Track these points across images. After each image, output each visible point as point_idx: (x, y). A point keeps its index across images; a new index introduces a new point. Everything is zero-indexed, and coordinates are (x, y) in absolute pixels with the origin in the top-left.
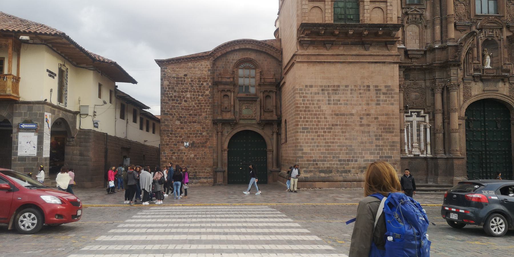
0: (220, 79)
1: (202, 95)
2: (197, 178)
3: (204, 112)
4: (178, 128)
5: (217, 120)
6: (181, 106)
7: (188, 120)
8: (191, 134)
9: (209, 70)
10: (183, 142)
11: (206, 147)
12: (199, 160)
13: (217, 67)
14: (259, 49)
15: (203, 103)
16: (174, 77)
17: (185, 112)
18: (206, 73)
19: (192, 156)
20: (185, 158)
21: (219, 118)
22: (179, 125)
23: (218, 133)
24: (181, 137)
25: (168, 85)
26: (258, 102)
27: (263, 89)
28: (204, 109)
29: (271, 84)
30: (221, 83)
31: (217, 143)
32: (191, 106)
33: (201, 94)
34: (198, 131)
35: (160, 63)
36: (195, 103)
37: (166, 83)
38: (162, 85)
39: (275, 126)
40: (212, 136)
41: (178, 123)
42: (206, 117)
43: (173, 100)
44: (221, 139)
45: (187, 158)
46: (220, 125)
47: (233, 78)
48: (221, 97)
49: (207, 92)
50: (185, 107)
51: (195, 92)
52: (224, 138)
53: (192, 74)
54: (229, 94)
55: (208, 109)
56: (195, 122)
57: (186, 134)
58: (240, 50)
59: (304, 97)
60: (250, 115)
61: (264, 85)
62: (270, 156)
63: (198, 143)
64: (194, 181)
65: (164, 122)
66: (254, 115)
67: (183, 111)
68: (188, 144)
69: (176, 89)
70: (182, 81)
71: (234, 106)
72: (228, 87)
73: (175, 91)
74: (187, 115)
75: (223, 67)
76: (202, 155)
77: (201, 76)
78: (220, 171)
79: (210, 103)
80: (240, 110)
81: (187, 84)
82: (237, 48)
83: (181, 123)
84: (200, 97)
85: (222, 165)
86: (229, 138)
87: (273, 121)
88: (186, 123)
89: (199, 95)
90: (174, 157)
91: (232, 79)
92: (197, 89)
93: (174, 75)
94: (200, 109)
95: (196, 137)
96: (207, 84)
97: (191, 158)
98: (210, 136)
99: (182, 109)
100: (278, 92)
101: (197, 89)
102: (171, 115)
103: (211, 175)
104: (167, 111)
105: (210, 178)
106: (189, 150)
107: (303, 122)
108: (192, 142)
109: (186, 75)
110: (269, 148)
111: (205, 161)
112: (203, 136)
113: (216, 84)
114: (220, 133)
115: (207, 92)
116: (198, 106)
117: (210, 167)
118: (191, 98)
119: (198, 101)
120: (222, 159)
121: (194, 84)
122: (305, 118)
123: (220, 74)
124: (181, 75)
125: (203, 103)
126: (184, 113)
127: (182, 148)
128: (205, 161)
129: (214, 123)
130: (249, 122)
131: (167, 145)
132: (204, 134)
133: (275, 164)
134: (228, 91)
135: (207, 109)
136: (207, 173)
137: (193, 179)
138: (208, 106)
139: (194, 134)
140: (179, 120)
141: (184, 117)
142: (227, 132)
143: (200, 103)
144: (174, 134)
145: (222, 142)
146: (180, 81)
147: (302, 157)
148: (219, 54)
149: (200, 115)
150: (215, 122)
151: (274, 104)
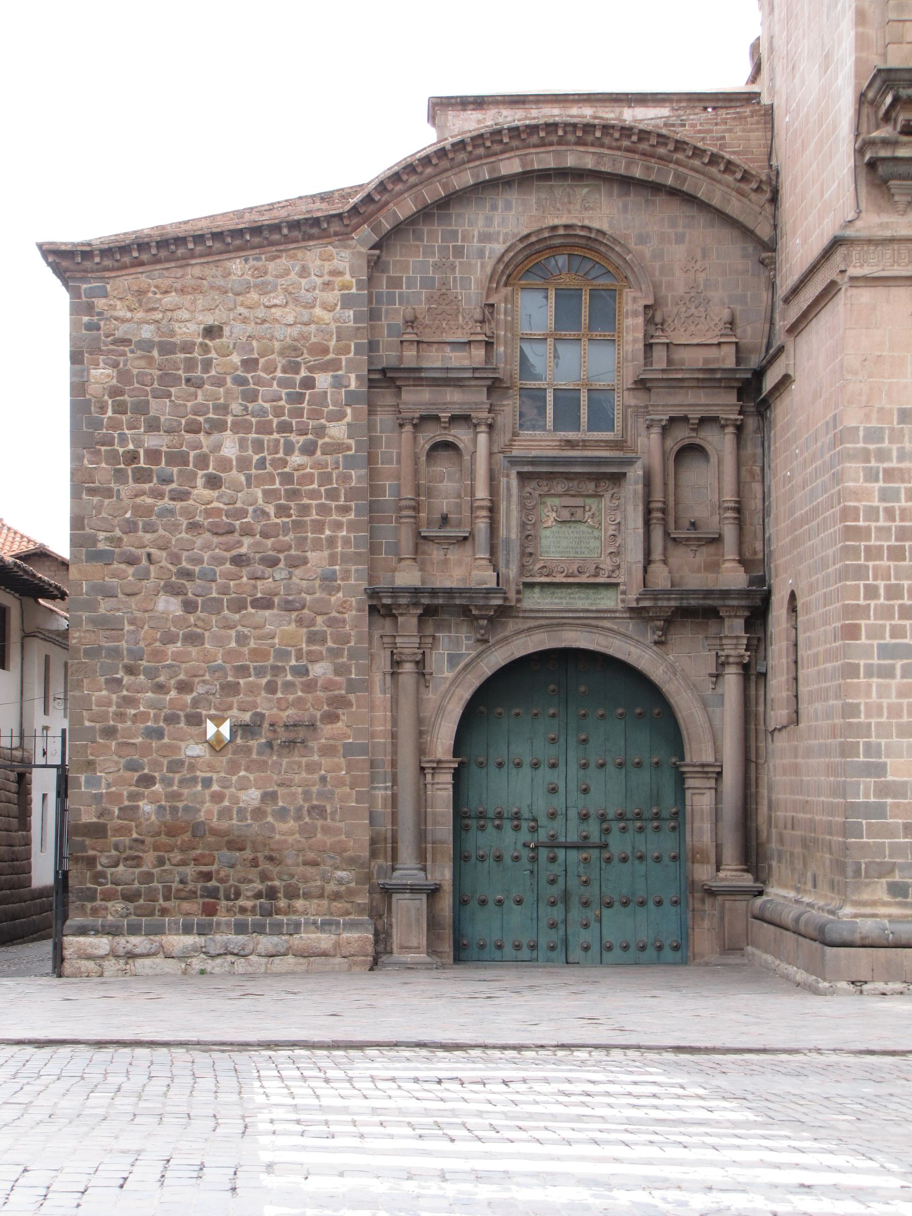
0: (410, 353)
1: (309, 449)
2: (277, 930)
3: (317, 545)
4: (169, 639)
5: (395, 592)
6: (188, 513)
7: (224, 590)
8: (243, 671)
9: (347, 301)
10: (196, 720)
12: (292, 824)
13: (395, 283)
14: (638, 173)
15: (313, 494)
16: (146, 346)
17: (207, 547)
18: (327, 316)
19: (252, 796)
20: (208, 812)
21: (408, 577)
22: (176, 621)
23: (396, 663)
24: (184, 687)
25: (115, 392)
26: (633, 486)
27: (668, 403)
28: (319, 527)
29: (710, 379)
30: (416, 377)
31: (395, 721)
32: (243, 513)
33: (298, 440)
34: (282, 654)
35: (67, 261)
36: (269, 495)
37: (101, 375)
38: (78, 388)
39: (736, 627)
40: (365, 686)
41: (170, 606)
42: (331, 569)
43: (142, 476)
44: (419, 702)
45: (224, 813)
46: (409, 622)
47: (489, 345)
48: (416, 458)
49: (337, 431)
50: (208, 513)
51: (265, 428)
52: (432, 696)
53: (250, 328)
54: (460, 435)
55: (344, 529)
56: (265, 604)
57: (213, 670)
58: (527, 179)
59: (889, 474)
60: (587, 564)
61: (676, 385)
62: (700, 801)
64: (266, 942)
65: (91, 606)
66: (607, 564)
67: (199, 542)
68: (225, 730)
69: (159, 408)
70: (190, 365)
71: (492, 510)
72: (455, 399)
73: (153, 426)
74: (220, 561)
75: (427, 283)
76: (307, 795)
77: (305, 337)
78: (414, 890)
79: (352, 494)
80: (528, 536)
81: (219, 382)
82: (511, 166)
83: (189, 606)
84: (296, 459)
85: (422, 855)
86: (466, 693)
87: (725, 594)
88: (214, 606)
89: (289, 448)
90: (146, 807)
91: (479, 353)
92: (278, 412)
93: (147, 332)
94: (298, 525)
95: (271, 688)
96: (338, 383)
97: (241, 811)
98: (352, 686)
99: (194, 527)
100: (751, 423)
101: (278, 412)
102: (132, 561)
103: (361, 910)
104: (109, 540)
105: (352, 926)
106: (233, 768)
107: (885, 613)
109: (211, 332)
110: (699, 751)
111: (326, 830)
112: (310, 687)
113: (385, 379)
114: (408, 667)
115: (337, 431)
116: (282, 511)
117: (352, 862)
118: (244, 463)
119: (287, 478)
120: (421, 817)
121: (259, 381)
122: (894, 592)
123: (411, 323)
124: (189, 329)
125: (313, 494)
126: (205, 549)
127: (195, 750)
128: (326, 830)
129: (373, 609)
130: (581, 601)
131: (110, 732)
132: (320, 670)
133: (730, 852)
134: (455, 419)
135: (338, 525)
136: (336, 896)
137: (259, 929)
138: (345, 510)
139: (260, 672)
140: (173, 590)
141: (203, 575)
142: (453, 660)
143: (293, 494)
144: (151, 673)
145: (420, 721)
146: (178, 362)
147: (879, 811)
148: (406, 207)
149: (295, 563)
150: (381, 607)
151: (729, 497)
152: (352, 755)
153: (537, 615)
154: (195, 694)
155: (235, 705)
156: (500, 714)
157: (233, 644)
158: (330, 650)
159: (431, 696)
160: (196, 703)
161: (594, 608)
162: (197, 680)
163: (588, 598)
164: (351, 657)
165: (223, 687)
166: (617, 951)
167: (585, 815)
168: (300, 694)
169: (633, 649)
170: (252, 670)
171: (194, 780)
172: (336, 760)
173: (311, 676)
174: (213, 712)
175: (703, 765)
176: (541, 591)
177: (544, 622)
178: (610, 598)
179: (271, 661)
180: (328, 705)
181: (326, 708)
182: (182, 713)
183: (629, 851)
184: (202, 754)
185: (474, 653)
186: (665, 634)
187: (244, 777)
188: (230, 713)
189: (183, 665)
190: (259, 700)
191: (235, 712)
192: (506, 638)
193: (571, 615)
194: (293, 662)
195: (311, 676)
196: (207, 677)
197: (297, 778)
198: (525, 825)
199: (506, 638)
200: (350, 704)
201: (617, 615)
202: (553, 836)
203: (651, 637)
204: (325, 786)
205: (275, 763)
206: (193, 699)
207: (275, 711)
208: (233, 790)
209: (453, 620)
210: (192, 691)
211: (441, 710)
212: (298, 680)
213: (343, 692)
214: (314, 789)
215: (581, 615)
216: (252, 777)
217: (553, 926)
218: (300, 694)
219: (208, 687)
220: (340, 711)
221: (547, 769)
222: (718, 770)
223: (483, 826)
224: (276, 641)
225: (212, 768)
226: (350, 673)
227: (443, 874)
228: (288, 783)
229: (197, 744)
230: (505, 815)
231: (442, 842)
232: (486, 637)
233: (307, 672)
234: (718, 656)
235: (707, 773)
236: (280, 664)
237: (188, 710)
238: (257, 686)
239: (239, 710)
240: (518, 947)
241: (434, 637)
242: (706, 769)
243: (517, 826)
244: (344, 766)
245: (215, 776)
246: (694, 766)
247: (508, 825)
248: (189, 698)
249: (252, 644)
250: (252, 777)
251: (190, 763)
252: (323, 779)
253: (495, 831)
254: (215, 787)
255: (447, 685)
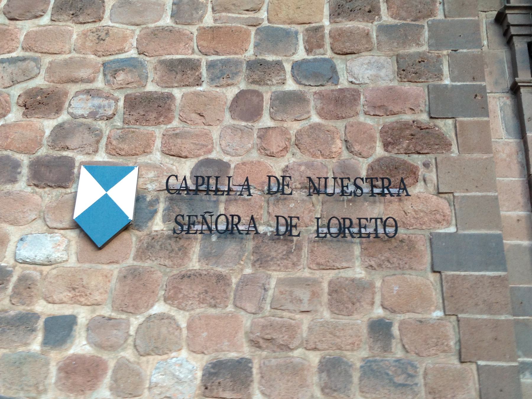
8: (182, 70)
10: (55, 174)
11: (384, 238)
24: (39, 103)
34: (274, 38)
63: (278, 189)
68: (124, 195)
95: (246, 107)
98: (442, 103)
106: (135, 288)
108: (185, 169)
112: (341, 103)
139: (222, 73)
152: (460, 266)
154: (64, 117)
155: (158, 143)
157: (167, 21)
158: (384, 29)
160: (61, 133)
162: (73, 89)
164: (438, 39)
165: (132, 103)
168: (315, 119)
170: (204, 70)
171: (25, 322)
172: (413, 277)
173: (344, 83)
174: (101, 157)
179: (250, 53)
180: (386, 145)
181: (379, 151)
182: (25, 160)
184: (56, 255)
187: (162, 317)
188: (142, 159)
189: (47, 60)
190: (215, 133)
191: (156, 157)
194: (301, 54)
195: (344, 83)
196: (100, 83)
197: (305, 322)
200: (444, 144)
204: (386, 348)
205: (245, 282)
206: (60, 126)
207: (255, 155)
208: (129, 354)
210: (58, 110)
212: (310, 92)
213: (424, 117)
214: (357, 357)
216: (182, 319)
218: (315, 119)
219: (97, 101)
220: (417, 160)
224: (263, 14)
225: (78, 290)
226: (439, 75)
228: (281, 338)
229: (51, 229)
233: (333, 76)
236: (270, 58)
237: (43, 152)
238: (214, 99)
239: (167, 153)
244: (436, 297)
245: (83, 315)
248: (48, 125)
249: (208, 20)
250: (182, 319)
251: (23, 279)
252: (380, 330)
254: (80, 346)
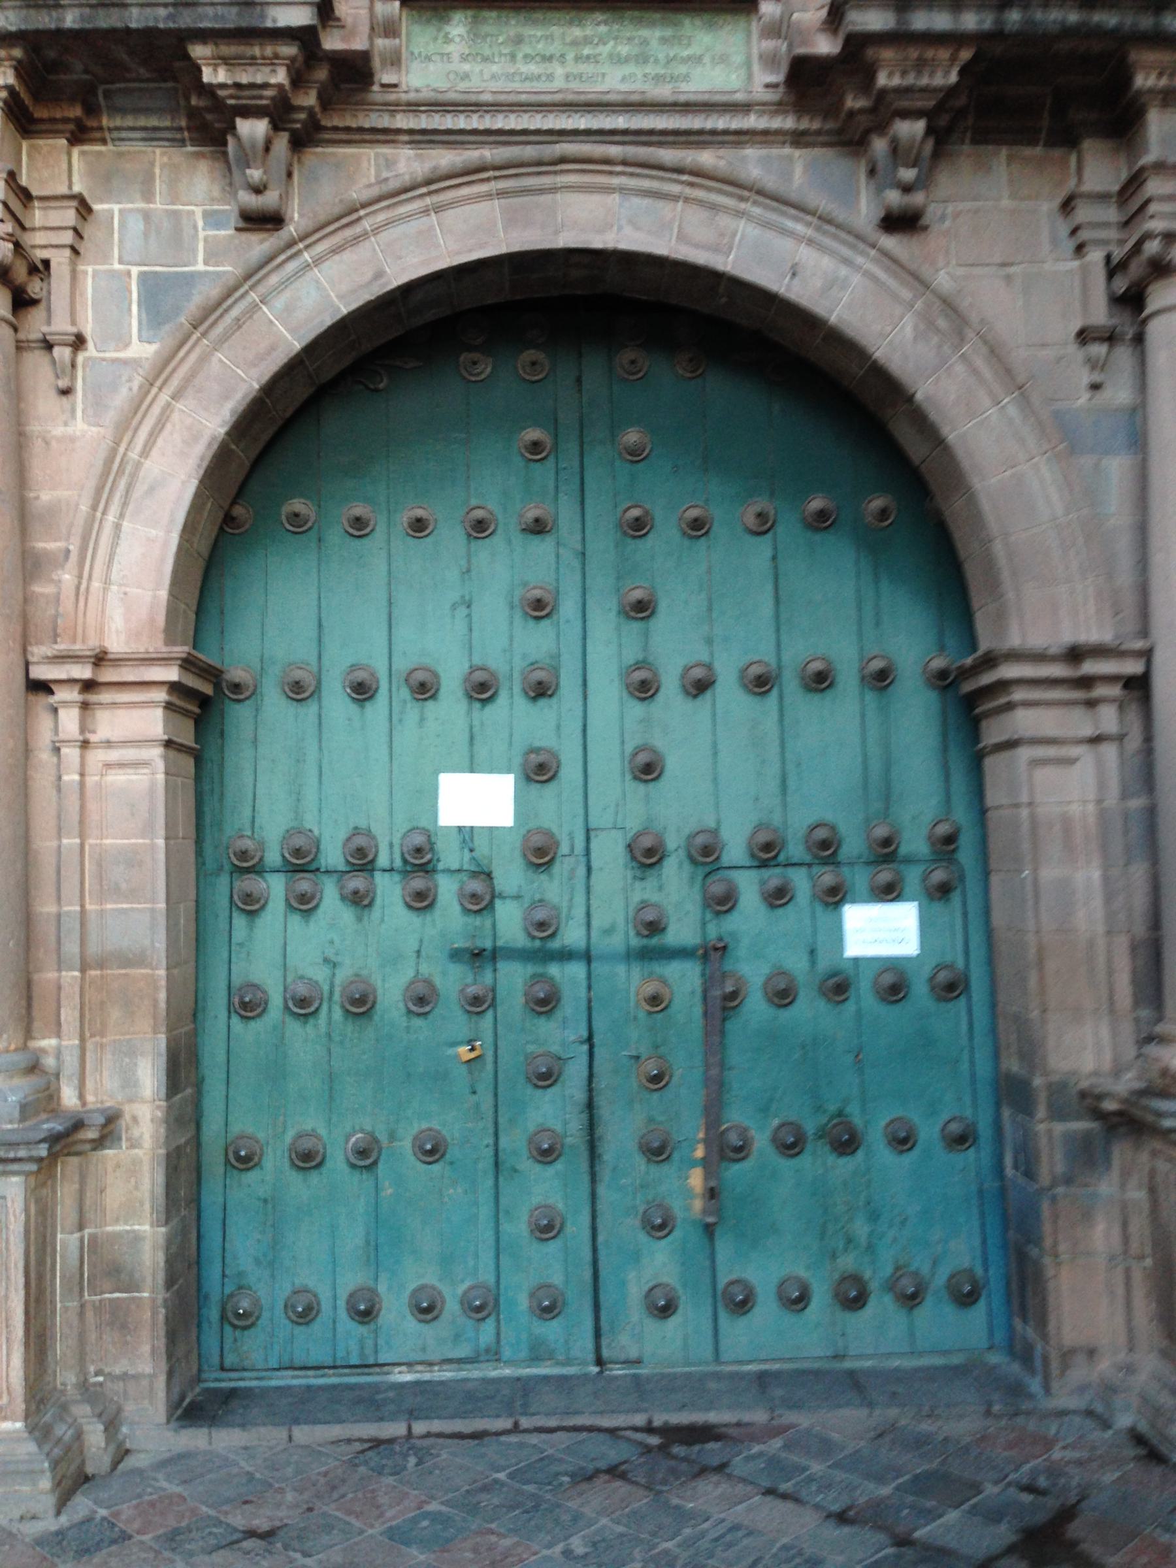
142: (158, 294)
153: (462, 122)
156: (359, 523)
159: (80, 426)
161: (663, 92)
163: (643, 59)
166: (766, 1307)
167: (650, 852)
169: (805, 254)
175: (1075, 654)
176: (475, 35)
177: (487, 154)
178: (723, 59)
183: (797, 964)
185: (228, 269)
186: (923, 183)
192: (350, 213)
193: (582, 122)
198: (447, 889)
199: (350, 213)
201: (752, 121)
202: (542, 925)
203: (865, 209)
209: (160, 157)
211: (113, 475)
215: (620, 122)
217: (547, 1228)
221: (521, 702)
222: (1133, 667)
223: (304, 898)
227: (129, 1081)
230: (383, 861)
231: (127, 960)
232: (270, 200)
234: (1113, 269)
235: (1086, 682)
240: (427, 1310)
241: (84, 208)
242: (1090, 667)
243: (420, 895)
246: (1039, 657)
247: (389, 890)
253: (347, 915)
255: (137, 381)
